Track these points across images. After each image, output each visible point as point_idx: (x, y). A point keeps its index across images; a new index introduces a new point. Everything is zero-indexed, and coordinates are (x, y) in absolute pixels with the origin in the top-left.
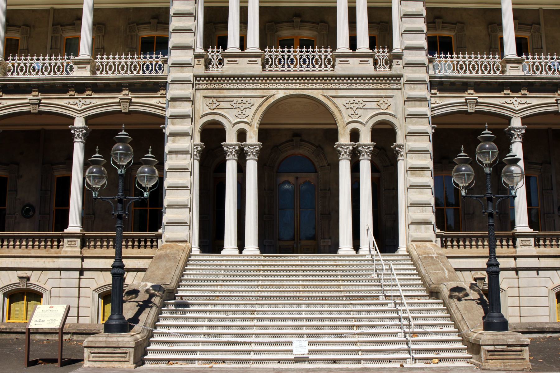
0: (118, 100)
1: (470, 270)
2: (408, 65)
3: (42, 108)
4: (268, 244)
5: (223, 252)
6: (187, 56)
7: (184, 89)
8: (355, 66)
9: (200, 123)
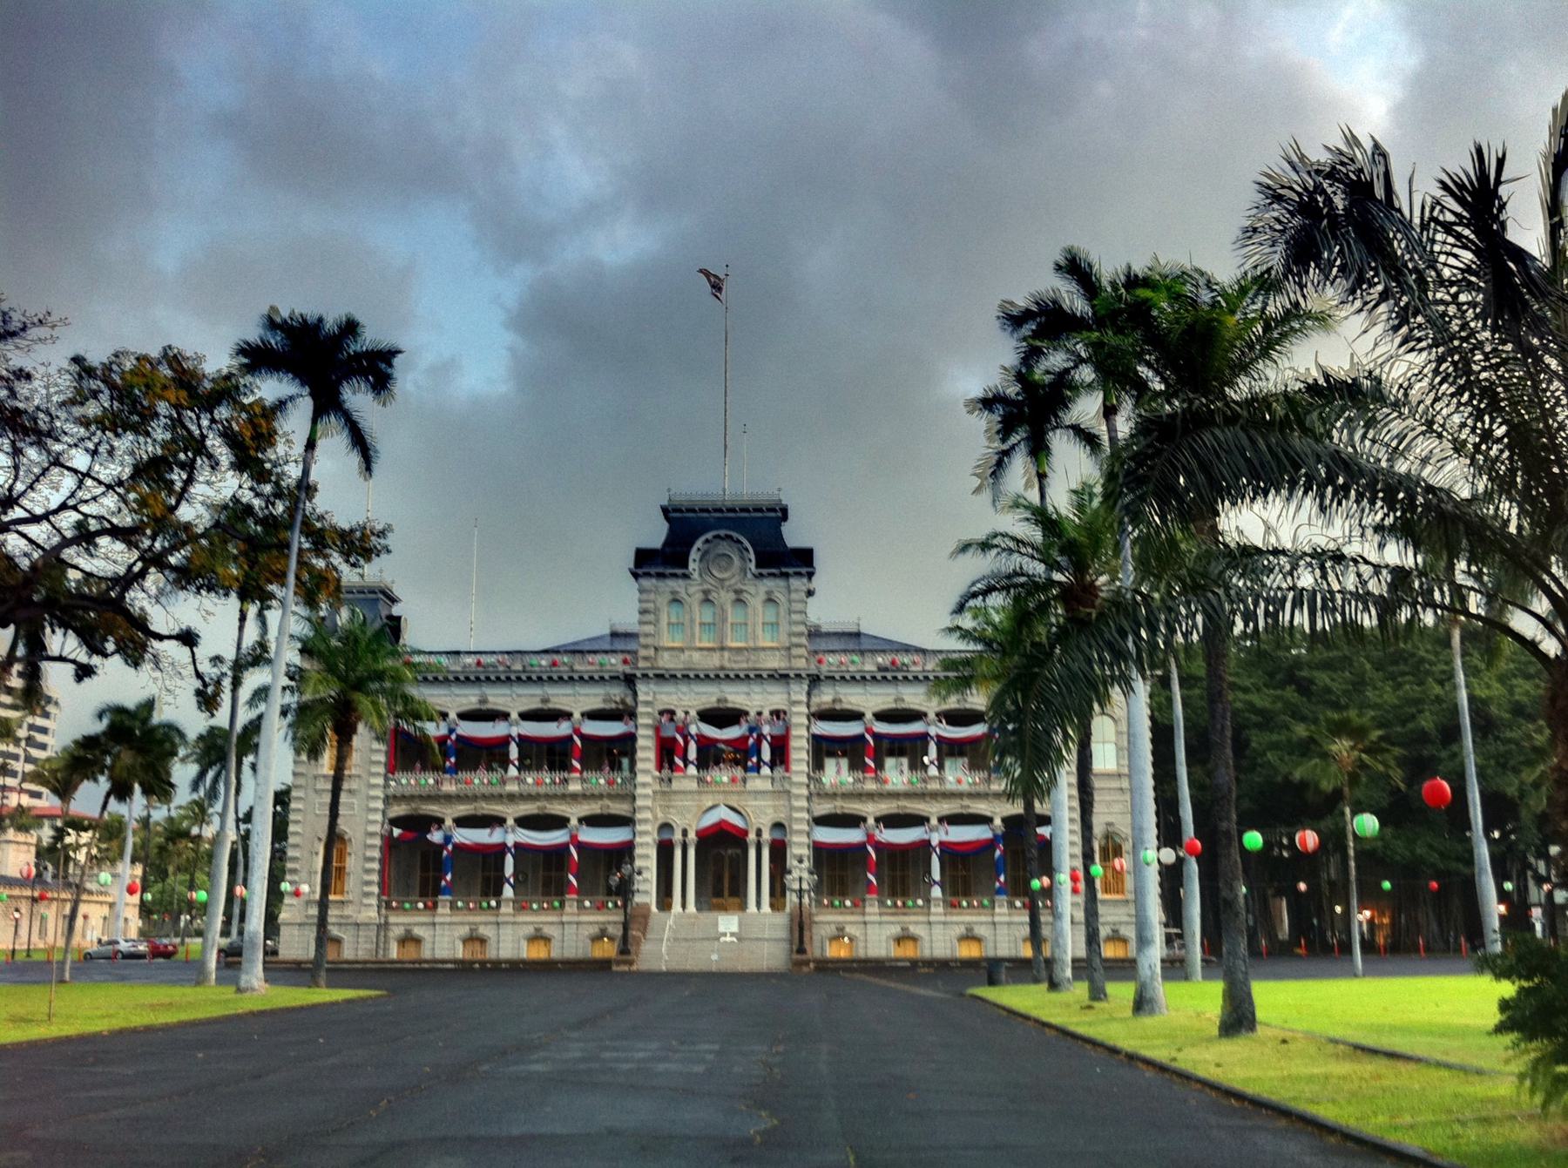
6: (648, 779)
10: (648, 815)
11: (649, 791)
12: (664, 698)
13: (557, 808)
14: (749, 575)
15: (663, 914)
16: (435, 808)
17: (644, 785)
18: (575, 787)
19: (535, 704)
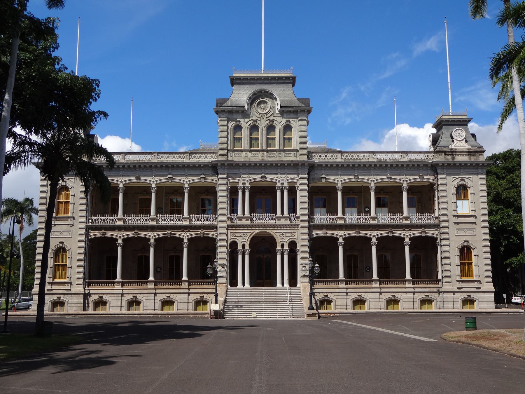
1: (323, 293)
2: (302, 221)
4: (253, 284)
8: (283, 221)
9: (229, 242)
14: (277, 112)
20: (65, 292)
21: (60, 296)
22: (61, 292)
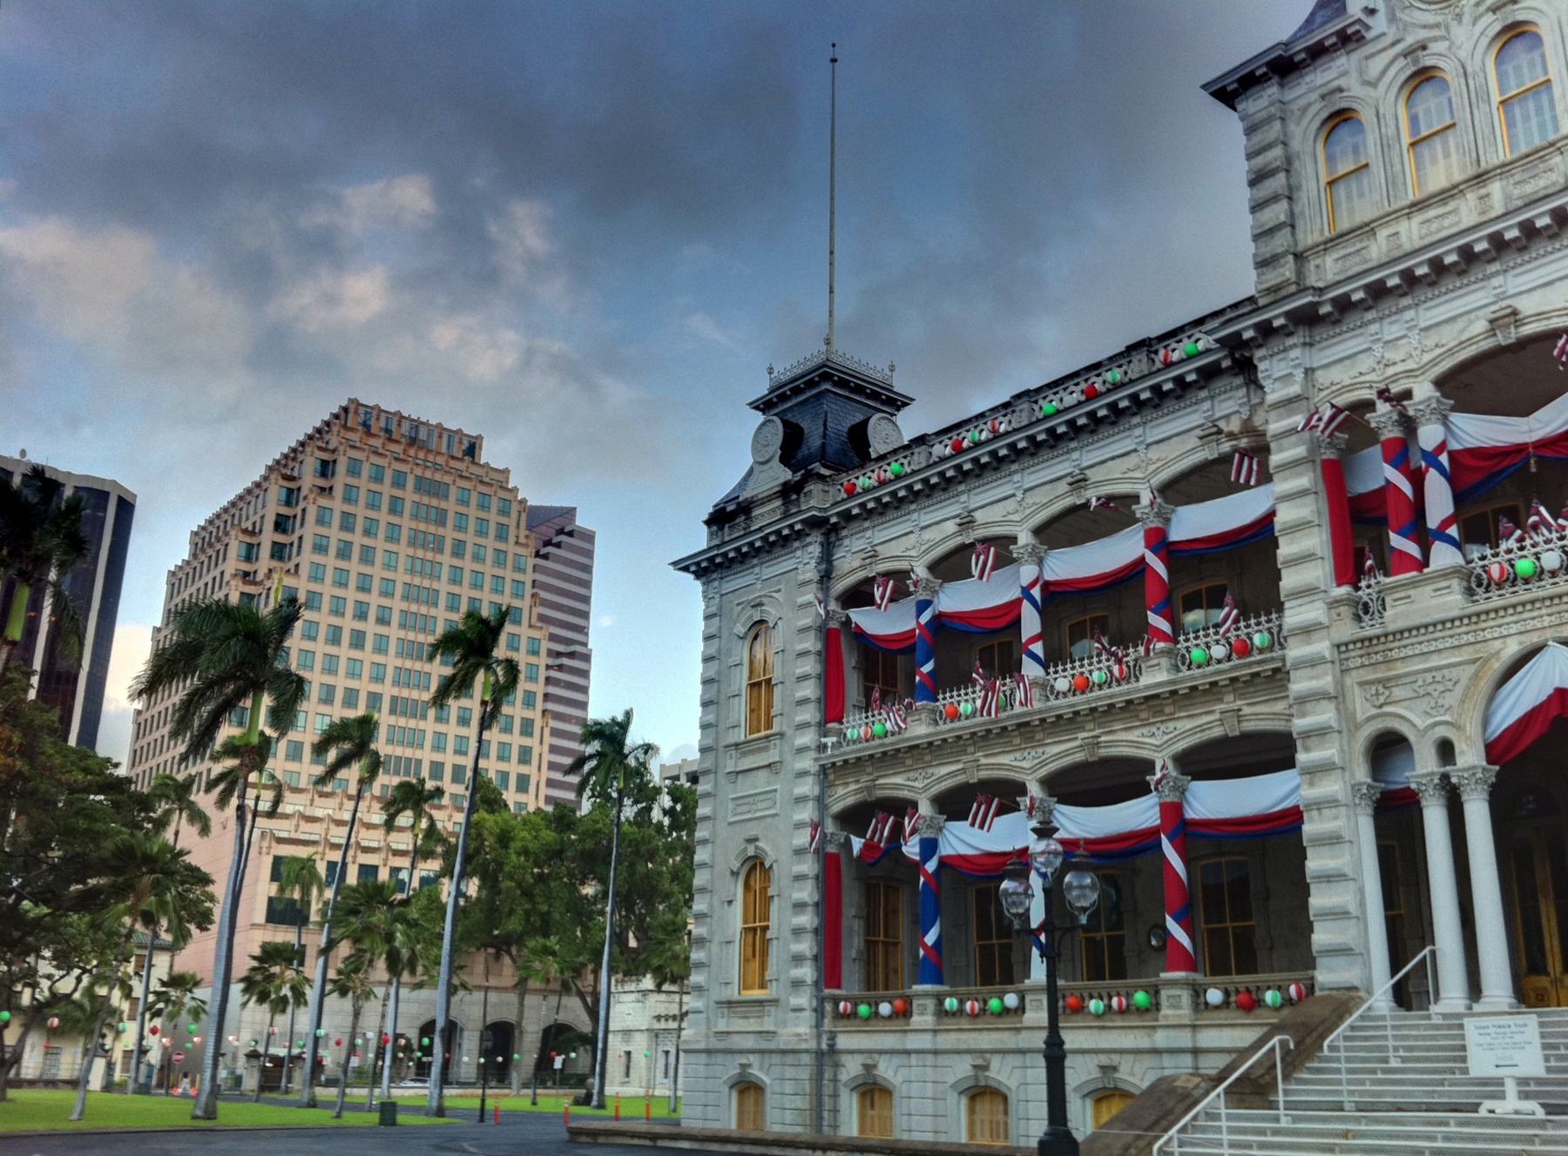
0: (1217, 716)
3: (1103, 752)
5: (1435, 1009)
7: (1317, 677)
10: (1324, 715)
11: (1321, 646)
12: (1342, 375)
13: (1127, 741)
15: (1413, 1018)
16: (898, 780)
17: (1307, 631)
18: (1155, 676)
19: (1059, 500)
20: (764, 1045)
21: (752, 1058)
22: (749, 1042)
